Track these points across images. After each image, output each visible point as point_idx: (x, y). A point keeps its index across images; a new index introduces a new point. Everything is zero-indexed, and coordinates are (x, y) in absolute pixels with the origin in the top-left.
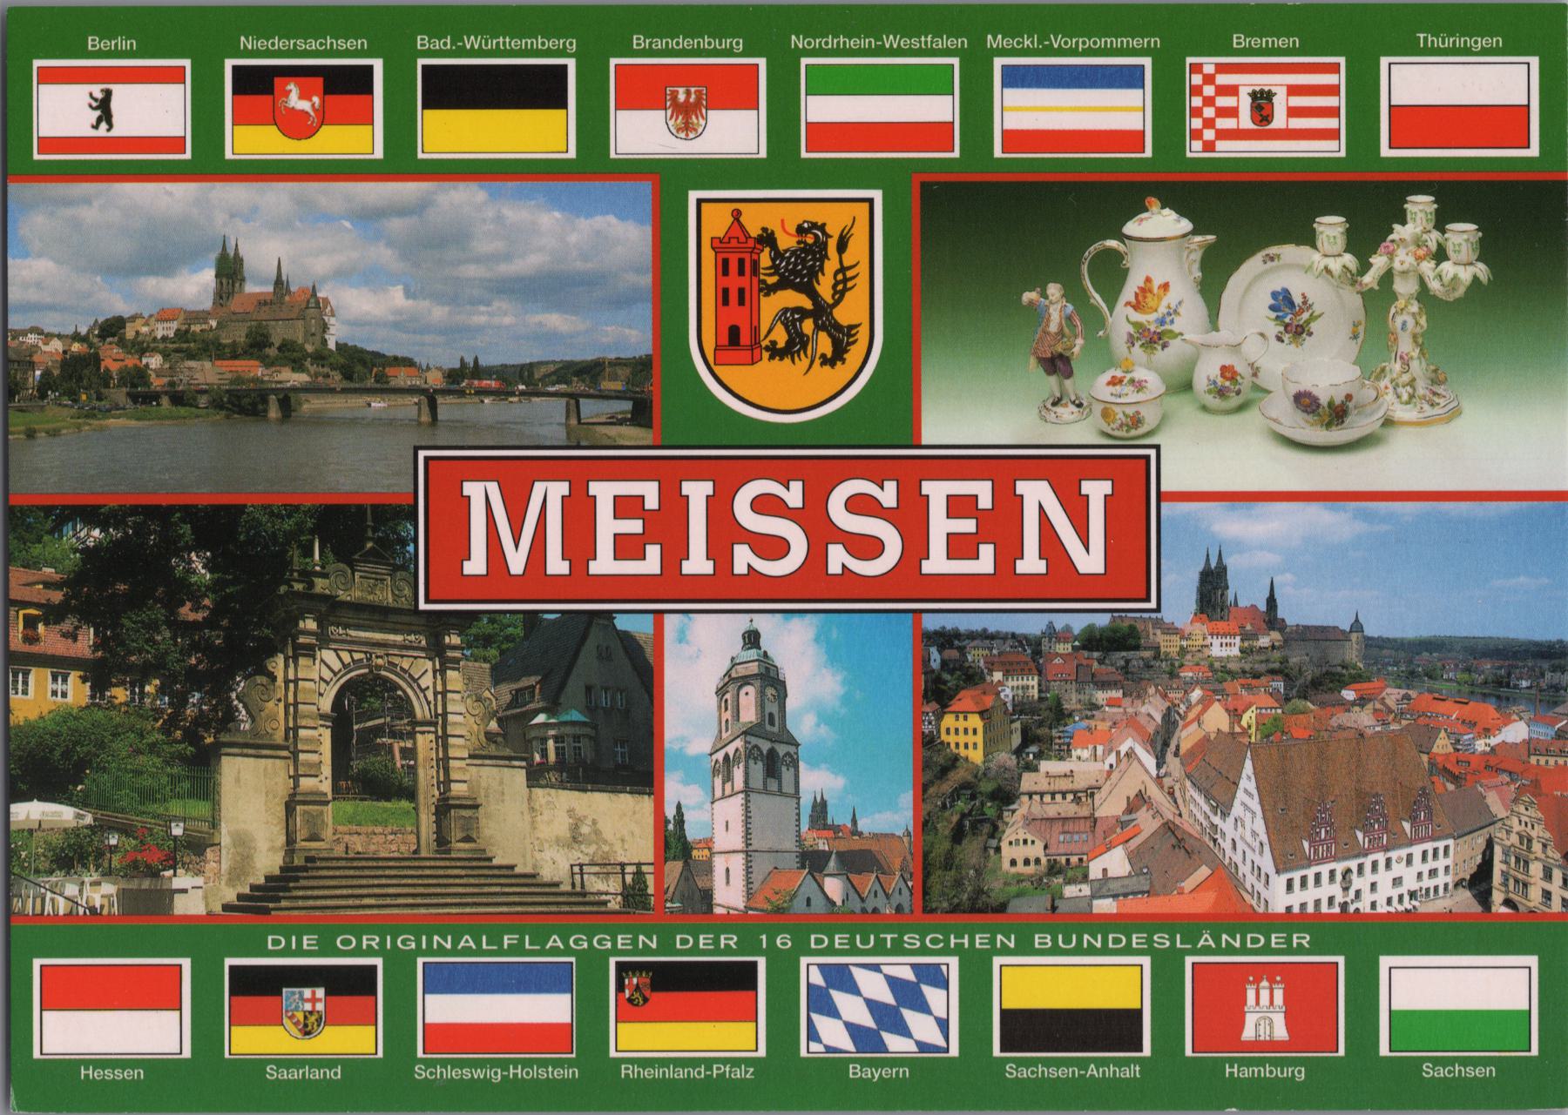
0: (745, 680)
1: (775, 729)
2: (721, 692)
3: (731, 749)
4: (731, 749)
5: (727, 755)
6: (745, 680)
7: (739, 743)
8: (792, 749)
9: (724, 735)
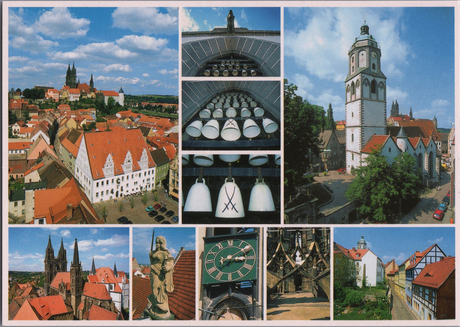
1: (376, 71)
2: (351, 54)
3: (355, 80)
4: (355, 80)
7: (358, 77)
9: (352, 73)
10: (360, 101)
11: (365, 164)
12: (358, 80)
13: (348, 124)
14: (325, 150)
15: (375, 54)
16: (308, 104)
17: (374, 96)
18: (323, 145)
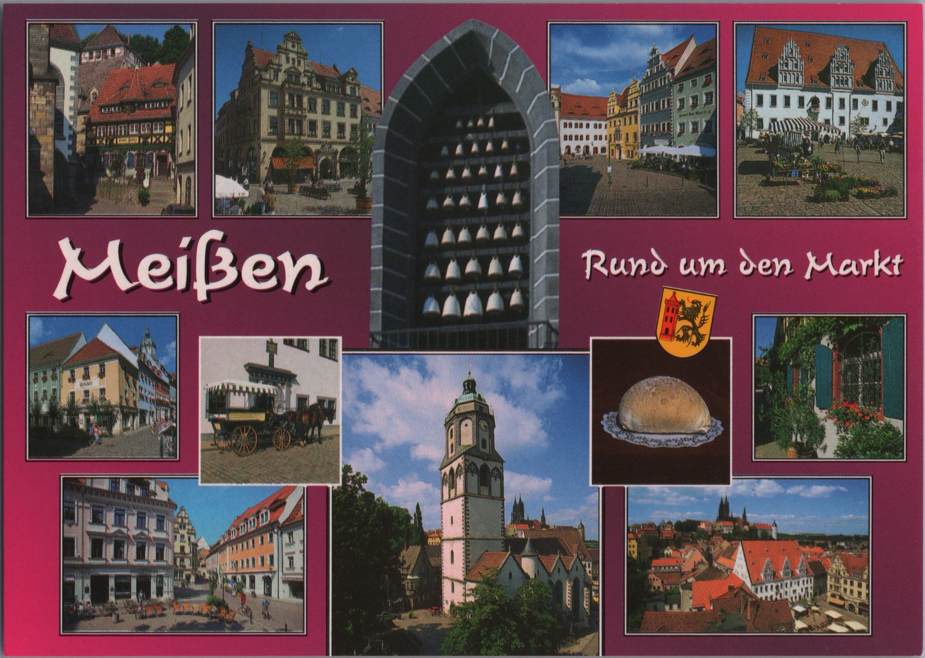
0: (464, 416)
1: (487, 451)
2: (448, 424)
3: (454, 465)
4: (454, 465)
5: (452, 470)
6: (464, 416)
7: (460, 460)
8: (499, 465)
9: (450, 455)
10: (462, 498)
11: (471, 599)
12: (459, 465)
13: (445, 535)
14: (409, 577)
15: (486, 424)
16: (383, 505)
17: (485, 492)
18: (408, 569)
